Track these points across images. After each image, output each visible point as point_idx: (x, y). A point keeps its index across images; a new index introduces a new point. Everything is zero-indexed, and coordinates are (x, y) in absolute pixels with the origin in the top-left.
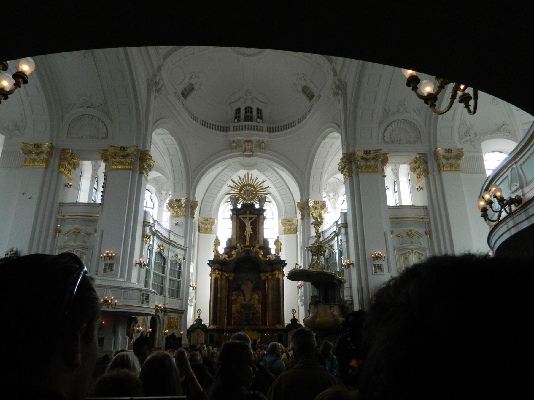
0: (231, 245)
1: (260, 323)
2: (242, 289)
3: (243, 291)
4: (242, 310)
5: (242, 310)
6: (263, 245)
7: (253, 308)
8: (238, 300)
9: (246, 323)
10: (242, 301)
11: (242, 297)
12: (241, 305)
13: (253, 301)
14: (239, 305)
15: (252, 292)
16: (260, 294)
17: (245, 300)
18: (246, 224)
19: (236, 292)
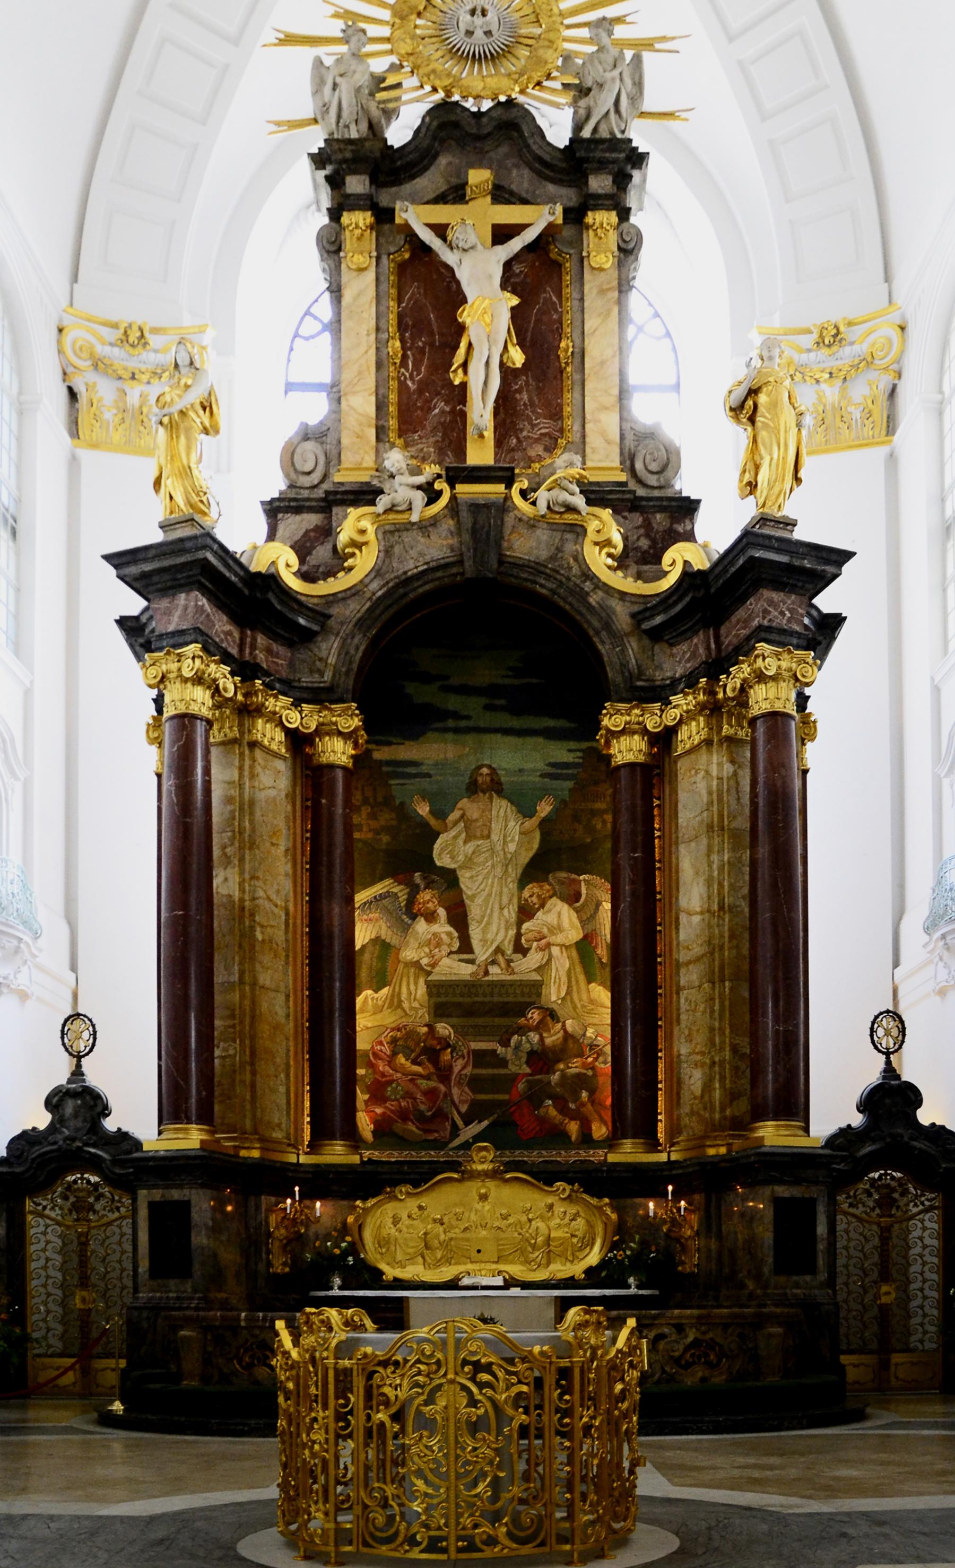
0: (338, 478)
1: (600, 1131)
2: (442, 859)
3: (450, 879)
4: (444, 1029)
5: (444, 1029)
6: (623, 477)
7: (534, 1016)
8: (409, 954)
9: (476, 1128)
10: (446, 961)
11: (443, 928)
12: (434, 988)
13: (535, 958)
14: (422, 990)
15: (523, 882)
16: (598, 904)
17: (466, 946)
18: (463, 275)
19: (388, 882)
